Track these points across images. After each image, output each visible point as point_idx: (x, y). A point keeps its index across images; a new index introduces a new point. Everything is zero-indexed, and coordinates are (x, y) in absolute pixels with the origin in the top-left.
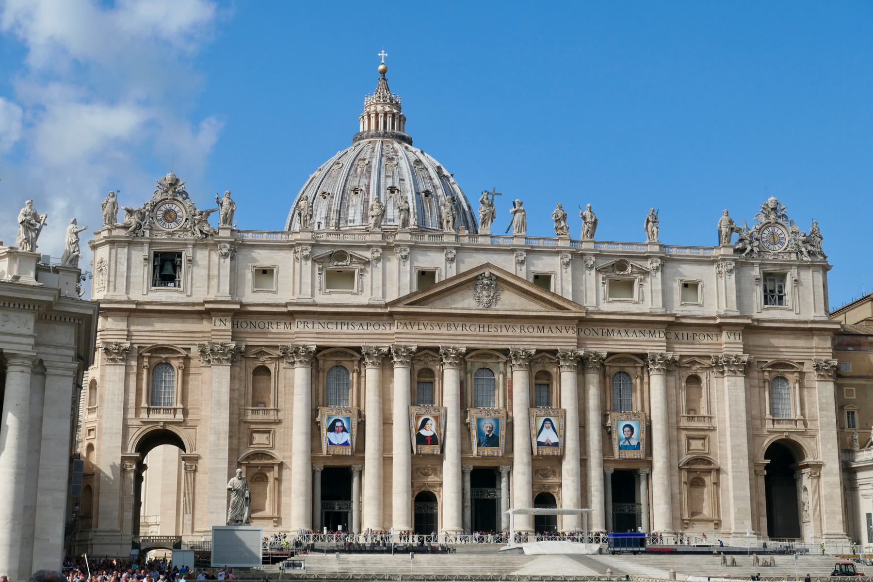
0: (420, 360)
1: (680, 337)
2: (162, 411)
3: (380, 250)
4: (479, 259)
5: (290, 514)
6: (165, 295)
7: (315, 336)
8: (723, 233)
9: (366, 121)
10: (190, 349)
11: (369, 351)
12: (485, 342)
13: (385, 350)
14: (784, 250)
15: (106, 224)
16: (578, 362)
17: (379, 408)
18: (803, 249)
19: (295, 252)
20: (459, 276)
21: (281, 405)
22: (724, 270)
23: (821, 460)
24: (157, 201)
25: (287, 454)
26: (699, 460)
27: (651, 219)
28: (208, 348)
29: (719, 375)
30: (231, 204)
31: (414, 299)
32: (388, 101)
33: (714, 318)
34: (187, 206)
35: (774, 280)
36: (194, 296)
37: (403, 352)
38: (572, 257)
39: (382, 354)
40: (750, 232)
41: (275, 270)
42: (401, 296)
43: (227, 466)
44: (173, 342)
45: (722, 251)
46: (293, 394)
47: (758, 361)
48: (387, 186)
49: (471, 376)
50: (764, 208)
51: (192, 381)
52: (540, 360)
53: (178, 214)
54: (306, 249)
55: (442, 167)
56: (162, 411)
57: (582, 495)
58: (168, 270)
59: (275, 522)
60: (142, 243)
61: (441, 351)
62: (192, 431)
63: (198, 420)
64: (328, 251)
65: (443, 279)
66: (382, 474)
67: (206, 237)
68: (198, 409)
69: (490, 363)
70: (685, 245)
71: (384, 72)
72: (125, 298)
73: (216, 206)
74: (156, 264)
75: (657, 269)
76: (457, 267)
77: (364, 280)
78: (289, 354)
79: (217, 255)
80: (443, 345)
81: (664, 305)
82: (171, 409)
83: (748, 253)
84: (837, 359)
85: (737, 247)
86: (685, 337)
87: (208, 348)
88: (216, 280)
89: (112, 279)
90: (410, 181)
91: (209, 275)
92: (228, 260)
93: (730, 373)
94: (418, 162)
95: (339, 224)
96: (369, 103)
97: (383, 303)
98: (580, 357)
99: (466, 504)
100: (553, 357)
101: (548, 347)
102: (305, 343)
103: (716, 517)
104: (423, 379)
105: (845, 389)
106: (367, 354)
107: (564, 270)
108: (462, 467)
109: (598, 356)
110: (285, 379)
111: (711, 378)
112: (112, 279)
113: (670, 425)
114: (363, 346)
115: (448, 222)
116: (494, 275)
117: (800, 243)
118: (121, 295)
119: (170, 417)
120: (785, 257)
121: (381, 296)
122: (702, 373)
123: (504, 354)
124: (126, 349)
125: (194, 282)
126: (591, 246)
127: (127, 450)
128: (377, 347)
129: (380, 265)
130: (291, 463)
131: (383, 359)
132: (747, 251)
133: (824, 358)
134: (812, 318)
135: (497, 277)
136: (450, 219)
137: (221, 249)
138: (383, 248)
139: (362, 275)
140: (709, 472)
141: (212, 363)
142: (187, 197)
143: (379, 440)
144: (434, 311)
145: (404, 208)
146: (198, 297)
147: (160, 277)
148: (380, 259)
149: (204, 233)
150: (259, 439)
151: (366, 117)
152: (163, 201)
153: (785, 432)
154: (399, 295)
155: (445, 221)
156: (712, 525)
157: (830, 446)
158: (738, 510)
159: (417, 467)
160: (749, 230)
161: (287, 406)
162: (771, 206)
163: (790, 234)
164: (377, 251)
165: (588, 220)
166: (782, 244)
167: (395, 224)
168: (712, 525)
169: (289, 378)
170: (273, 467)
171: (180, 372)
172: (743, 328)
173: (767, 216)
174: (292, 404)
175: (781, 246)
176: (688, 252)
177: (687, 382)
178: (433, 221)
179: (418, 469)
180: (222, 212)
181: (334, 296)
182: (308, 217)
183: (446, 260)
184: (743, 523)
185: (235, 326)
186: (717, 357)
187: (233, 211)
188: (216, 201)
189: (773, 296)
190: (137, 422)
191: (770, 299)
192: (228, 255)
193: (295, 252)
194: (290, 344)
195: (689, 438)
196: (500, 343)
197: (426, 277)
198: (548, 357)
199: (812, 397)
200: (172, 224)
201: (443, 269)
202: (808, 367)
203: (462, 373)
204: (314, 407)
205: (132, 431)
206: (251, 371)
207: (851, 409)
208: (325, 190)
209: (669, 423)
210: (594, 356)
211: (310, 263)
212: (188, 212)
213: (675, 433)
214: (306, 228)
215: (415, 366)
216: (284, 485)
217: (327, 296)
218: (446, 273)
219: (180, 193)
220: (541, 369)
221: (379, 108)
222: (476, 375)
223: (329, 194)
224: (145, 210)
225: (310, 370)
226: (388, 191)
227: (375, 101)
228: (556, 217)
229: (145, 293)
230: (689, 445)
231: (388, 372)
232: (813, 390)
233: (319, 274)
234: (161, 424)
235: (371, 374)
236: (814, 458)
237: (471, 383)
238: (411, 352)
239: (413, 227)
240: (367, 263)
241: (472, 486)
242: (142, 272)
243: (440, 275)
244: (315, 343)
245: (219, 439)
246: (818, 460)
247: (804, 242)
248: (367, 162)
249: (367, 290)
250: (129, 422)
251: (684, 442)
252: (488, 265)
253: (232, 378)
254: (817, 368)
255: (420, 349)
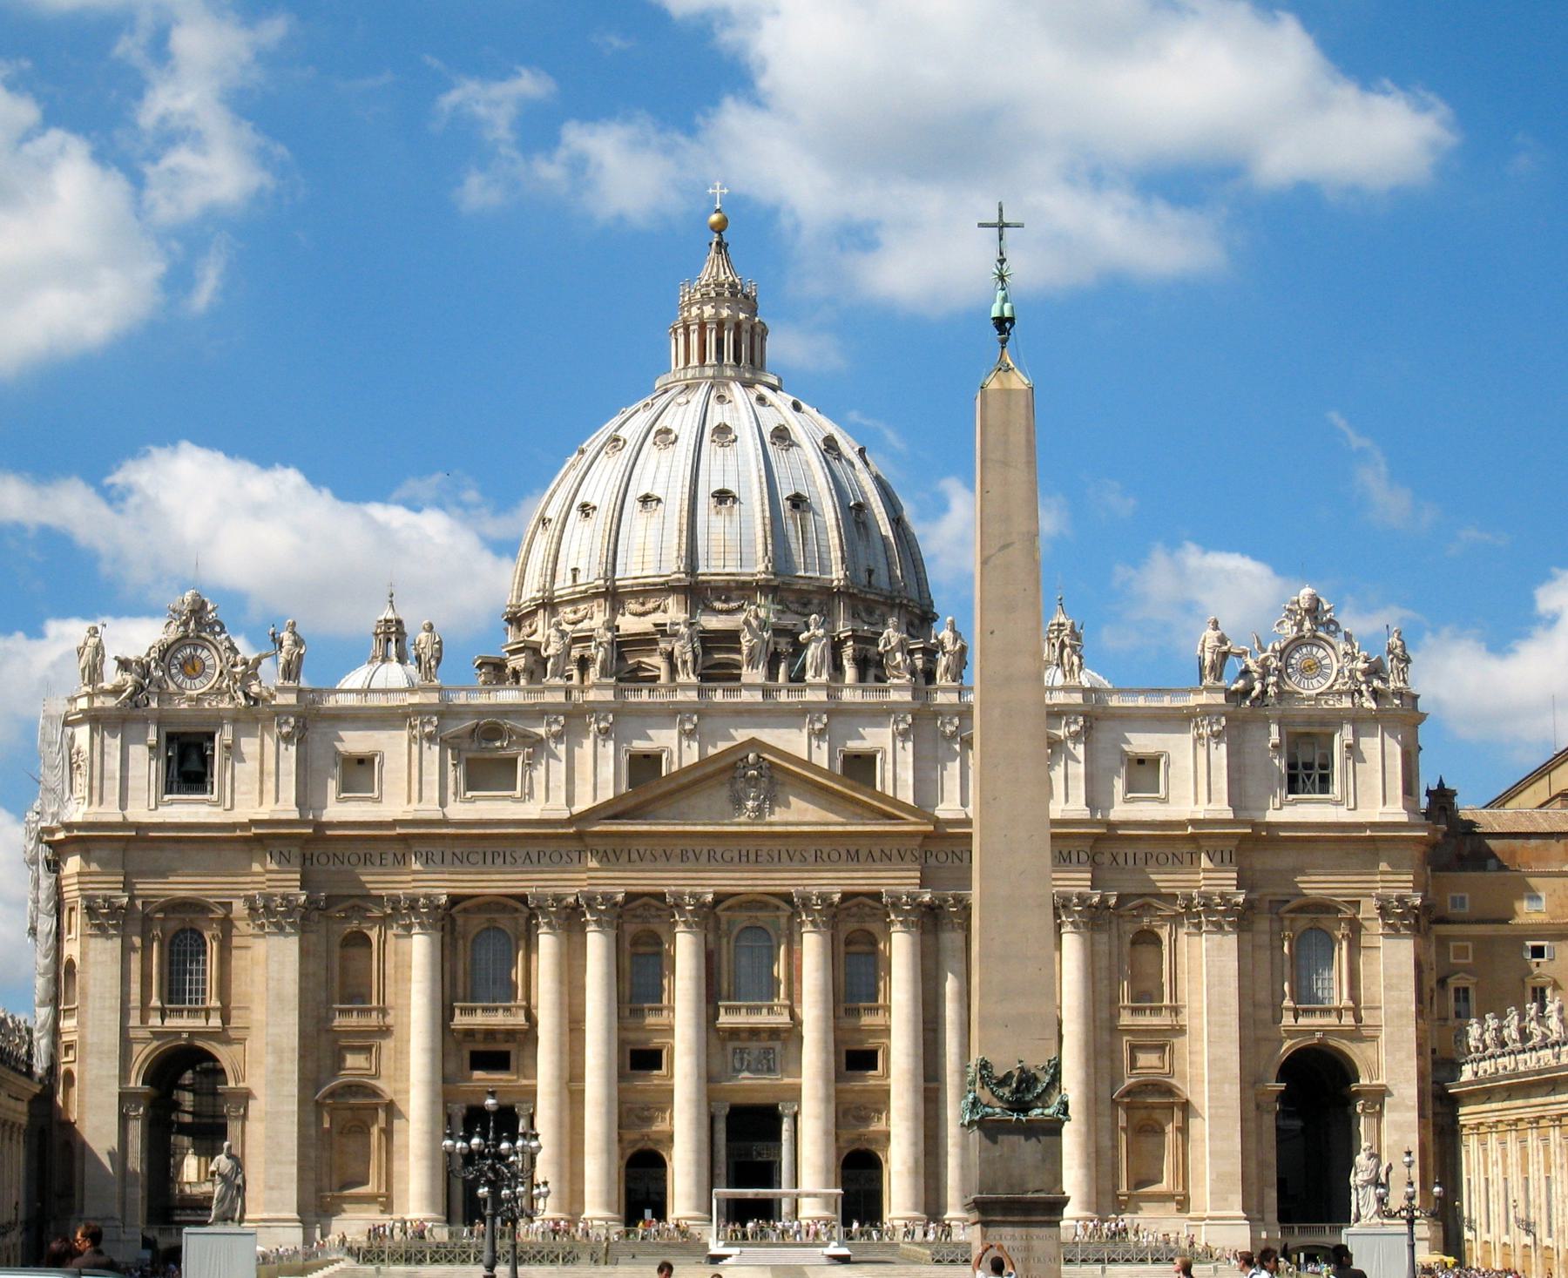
0: (635, 916)
1: (1121, 860)
2: (185, 1013)
3: (561, 718)
4: (742, 735)
5: (407, 1190)
6: (187, 810)
7: (447, 877)
8: (1207, 662)
9: (681, 340)
10: (231, 903)
11: (541, 904)
12: (750, 882)
13: (571, 900)
14: (1329, 688)
15: (85, 685)
16: (923, 915)
17: (561, 1004)
18: (1364, 687)
19: (412, 727)
20: (704, 761)
21: (390, 999)
22: (1206, 731)
23: (1384, 1082)
24: (170, 641)
25: (400, 1086)
26: (1150, 1087)
27: (1067, 641)
28: (260, 903)
29: (1192, 930)
30: (298, 642)
31: (619, 808)
32: (727, 294)
33: (1181, 825)
34: (221, 649)
35: (1313, 744)
36: (236, 810)
37: (602, 904)
38: (913, 719)
39: (566, 907)
40: (1263, 656)
41: (377, 760)
42: (598, 802)
43: (296, 1108)
44: (202, 893)
45: (1204, 699)
46: (410, 980)
47: (1270, 902)
48: (712, 491)
49: (728, 943)
50: (1290, 610)
51: (238, 960)
52: (854, 910)
53: (207, 663)
54: (430, 722)
55: (838, 437)
56: (185, 1013)
57: (927, 1154)
58: (193, 765)
59: (381, 1204)
60: (145, 721)
61: (668, 899)
62: (237, 1048)
63: (248, 1028)
64: (470, 723)
65: (675, 768)
66: (567, 1120)
67: (256, 703)
68: (246, 1008)
69: (763, 917)
70: (1135, 686)
71: (719, 228)
72: (119, 819)
73: (271, 648)
74: (170, 754)
75: (1075, 737)
76: (702, 749)
77: (534, 774)
78: (402, 912)
79: (272, 738)
80: (673, 888)
81: (1089, 803)
82: (201, 1010)
83: (1257, 698)
84: (1420, 894)
85: (1233, 688)
86: (1130, 861)
87: (260, 903)
88: (273, 779)
89: (96, 783)
90: (760, 477)
91: (262, 772)
92: (293, 749)
93: (1210, 928)
94: (782, 435)
95: (614, 572)
96: (686, 299)
97: (566, 815)
98: (920, 904)
99: (717, 1171)
100: (878, 905)
101: (866, 888)
102: (429, 891)
103: (1180, 1189)
104: (642, 949)
105: (1452, 944)
106: (540, 907)
107: (899, 745)
108: (709, 1104)
109: (961, 901)
110: (396, 953)
111: (1179, 936)
112: (96, 783)
113: (1098, 1023)
114: (532, 894)
115: (685, 663)
116: (764, 759)
117: (1359, 674)
118: (110, 812)
119: (198, 1023)
120: (1331, 702)
121: (564, 801)
122: (1161, 927)
123: (786, 902)
124: (121, 907)
125: (236, 785)
126: (953, 698)
127: (129, 1082)
128: (555, 895)
129: (561, 750)
130: (408, 1101)
131: (568, 918)
132: (1254, 694)
133: (1395, 893)
134: (1377, 819)
135: (770, 762)
136: (689, 657)
137: (280, 726)
138: (567, 715)
139: (529, 764)
140: (1171, 1107)
141: (267, 930)
142: (222, 631)
143: (561, 1060)
144: (654, 828)
145: (605, 639)
146: (242, 814)
147: (179, 775)
148: (562, 736)
149: (251, 697)
150: (351, 1060)
151: (681, 331)
152: (182, 642)
153: (1318, 1031)
154: (595, 798)
155: (679, 660)
156: (1173, 1206)
157: (1402, 1055)
158: (1217, 1177)
159: (628, 1105)
160: (1264, 651)
161: (400, 1001)
162: (1305, 604)
163: (1341, 658)
164: (556, 721)
165: (949, 647)
166: (1327, 677)
167: (727, 570)
168: (1173, 1206)
169: (404, 953)
170: (377, 1109)
171: (214, 944)
172: (1236, 842)
173: (1300, 625)
174: (409, 997)
175: (1323, 681)
176: (1141, 701)
177: (1134, 943)
178: (808, 561)
179: (630, 1110)
180: (283, 657)
181: (480, 805)
182: (433, 663)
183: (680, 733)
184: (1226, 1200)
185: (308, 863)
186: (1189, 898)
187: (300, 656)
188: (271, 638)
189: (1309, 776)
190: (146, 1034)
191: (1304, 781)
192: (293, 737)
193: (412, 727)
194: (401, 892)
195: (1134, 1048)
196: (778, 882)
197: (644, 766)
198: (868, 906)
199: (1371, 964)
200: (197, 681)
201: (676, 750)
202: (1369, 908)
203: (711, 937)
204: (447, 1002)
205: (137, 1048)
206: (337, 940)
207: (1463, 984)
208: (587, 499)
209: (1094, 1021)
210: (952, 902)
211: (436, 749)
212: (224, 660)
213: (1106, 1037)
214: (431, 681)
215: (626, 926)
216: (397, 1139)
217: (467, 806)
218: (680, 758)
219: (211, 625)
220: (856, 926)
221: (709, 311)
222: (737, 939)
223: (594, 508)
224: (148, 659)
225: (438, 935)
226: (713, 501)
227: (698, 296)
228: (885, 646)
229: (153, 806)
230: (1133, 1060)
231: (576, 938)
232: (1374, 951)
233: (454, 765)
234: (185, 1036)
235: (547, 943)
236: (1371, 1079)
237: (728, 953)
238: (616, 904)
239: (764, 576)
240: (538, 744)
241: (728, 1140)
242: (144, 767)
243: (670, 763)
244: (445, 891)
245: (281, 1061)
246: (1379, 1082)
247: (1364, 673)
248: (672, 437)
249: (539, 791)
250: (132, 1034)
251: (1126, 1055)
252: (753, 743)
253: (304, 953)
254: (1384, 911)
255: (631, 897)
